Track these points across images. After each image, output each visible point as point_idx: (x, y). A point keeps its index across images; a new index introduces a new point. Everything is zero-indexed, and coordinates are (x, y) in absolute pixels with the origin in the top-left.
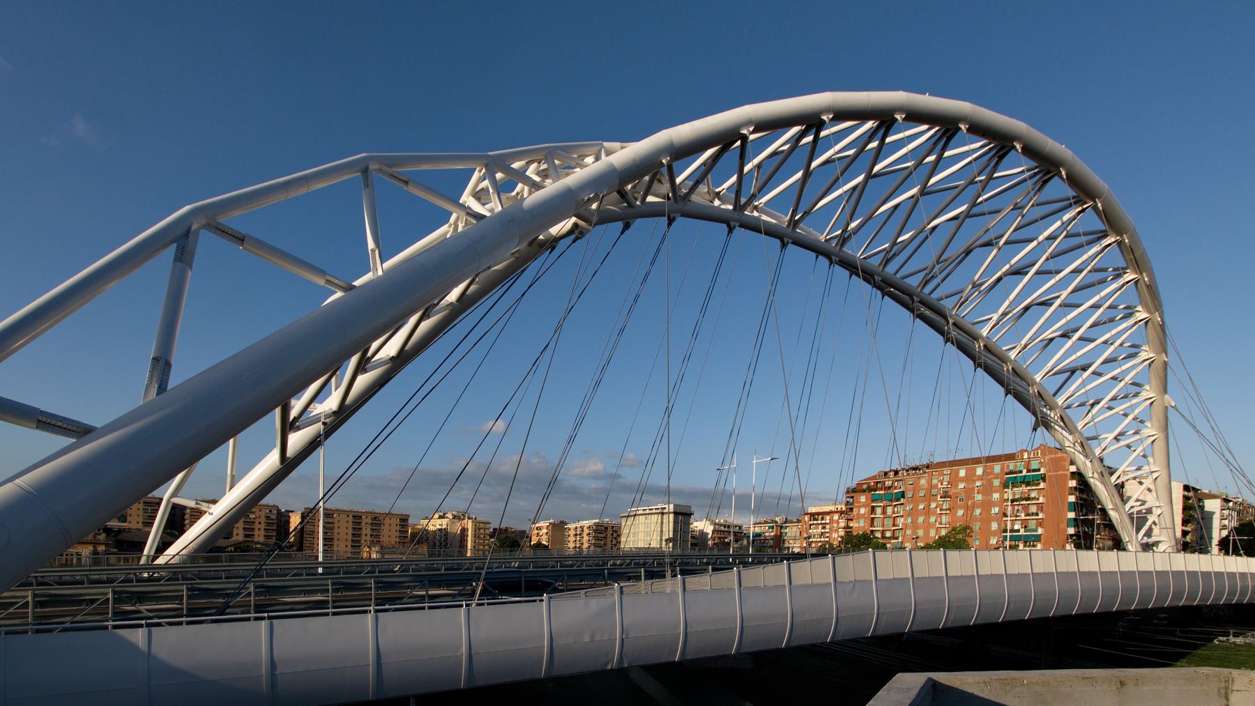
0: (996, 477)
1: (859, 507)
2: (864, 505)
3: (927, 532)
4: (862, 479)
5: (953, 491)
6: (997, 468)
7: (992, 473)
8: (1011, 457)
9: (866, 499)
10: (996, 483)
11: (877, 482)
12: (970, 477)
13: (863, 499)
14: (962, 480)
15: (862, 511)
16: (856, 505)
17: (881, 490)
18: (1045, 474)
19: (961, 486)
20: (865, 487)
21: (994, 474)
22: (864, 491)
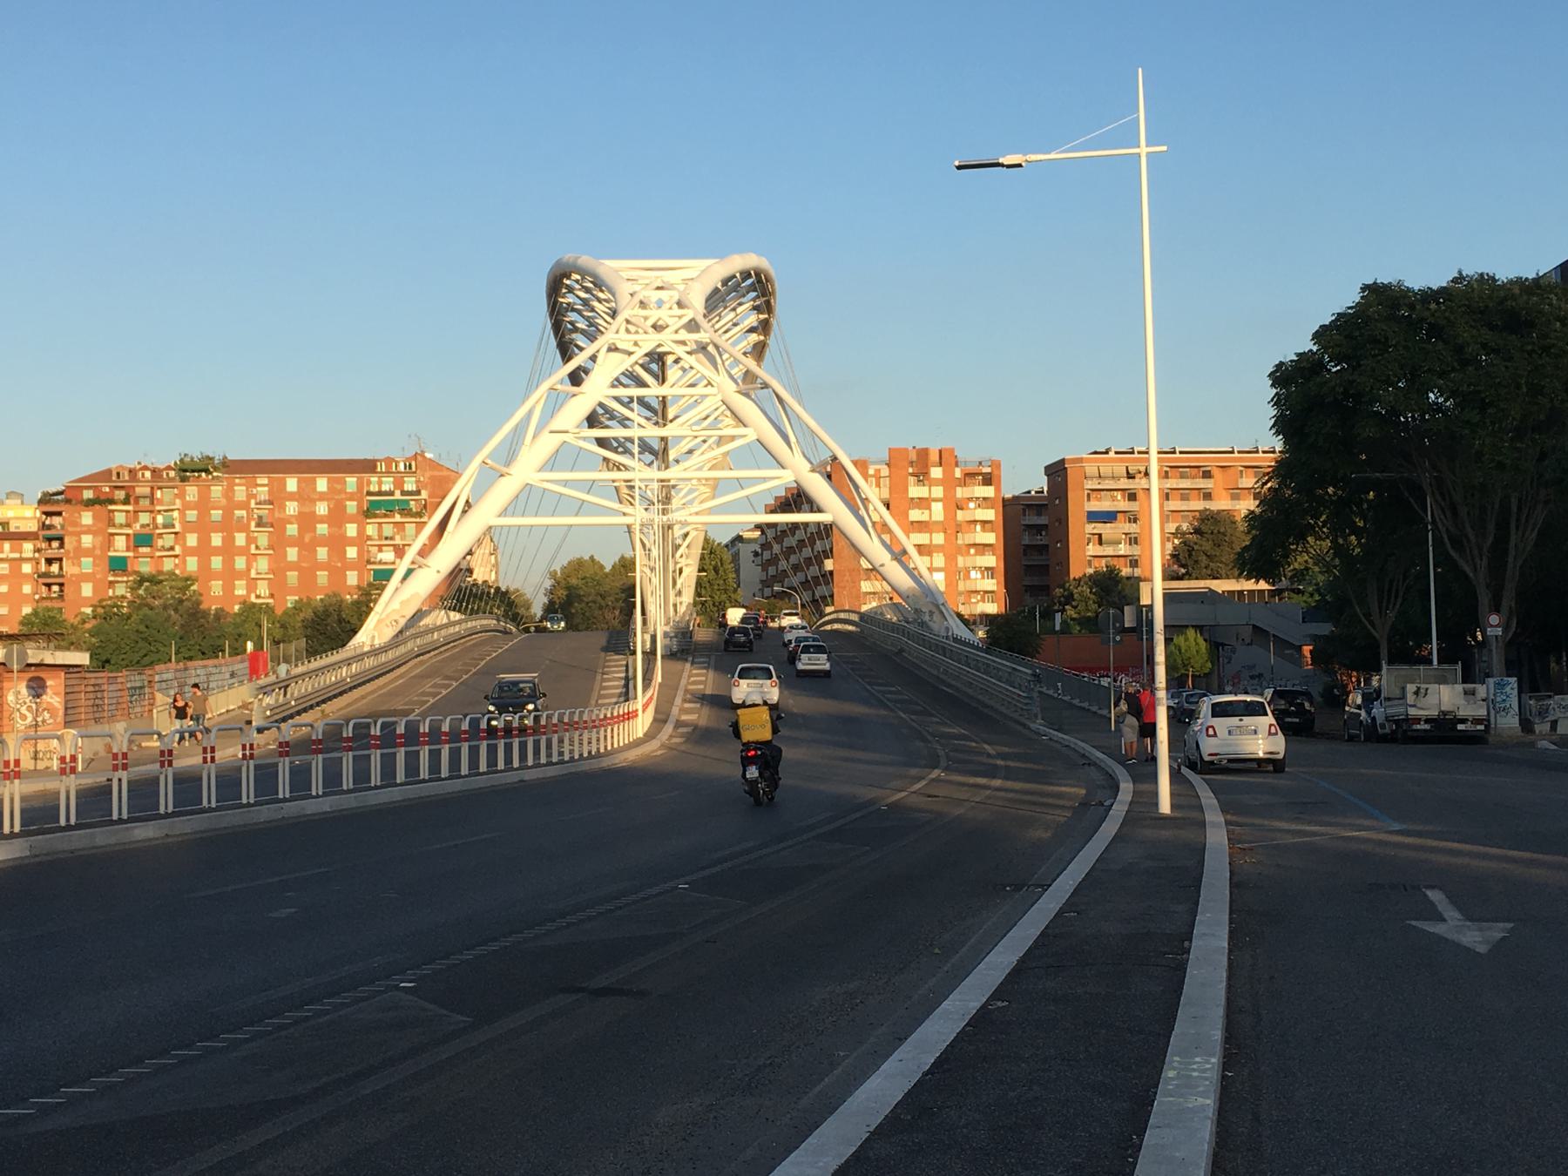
0: (351, 497)
1: (79, 534)
2: (88, 530)
3: (229, 588)
4: (73, 479)
5: (277, 515)
6: (351, 481)
7: (343, 491)
8: (368, 466)
9: (94, 517)
10: (352, 507)
11: (116, 487)
12: (306, 496)
13: (87, 518)
14: (292, 497)
15: (87, 540)
16: (70, 529)
17: (126, 502)
18: (425, 500)
19: (292, 508)
20: (88, 494)
21: (346, 493)
22: (89, 504)
